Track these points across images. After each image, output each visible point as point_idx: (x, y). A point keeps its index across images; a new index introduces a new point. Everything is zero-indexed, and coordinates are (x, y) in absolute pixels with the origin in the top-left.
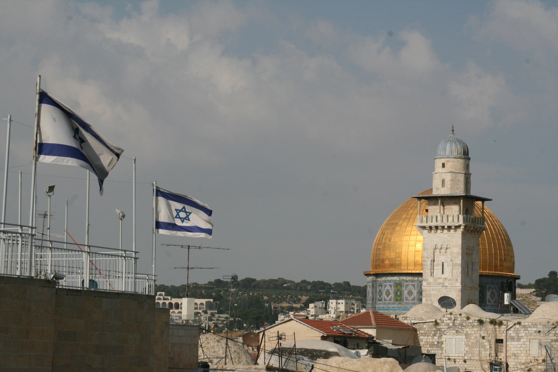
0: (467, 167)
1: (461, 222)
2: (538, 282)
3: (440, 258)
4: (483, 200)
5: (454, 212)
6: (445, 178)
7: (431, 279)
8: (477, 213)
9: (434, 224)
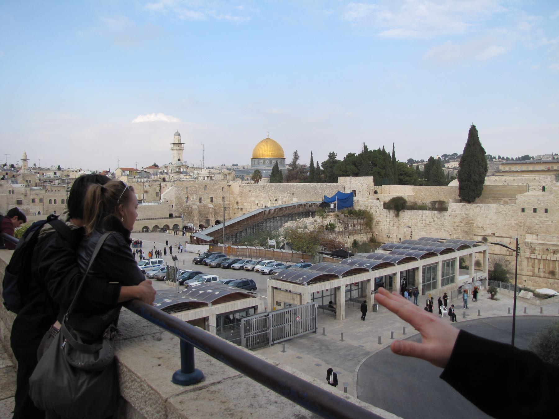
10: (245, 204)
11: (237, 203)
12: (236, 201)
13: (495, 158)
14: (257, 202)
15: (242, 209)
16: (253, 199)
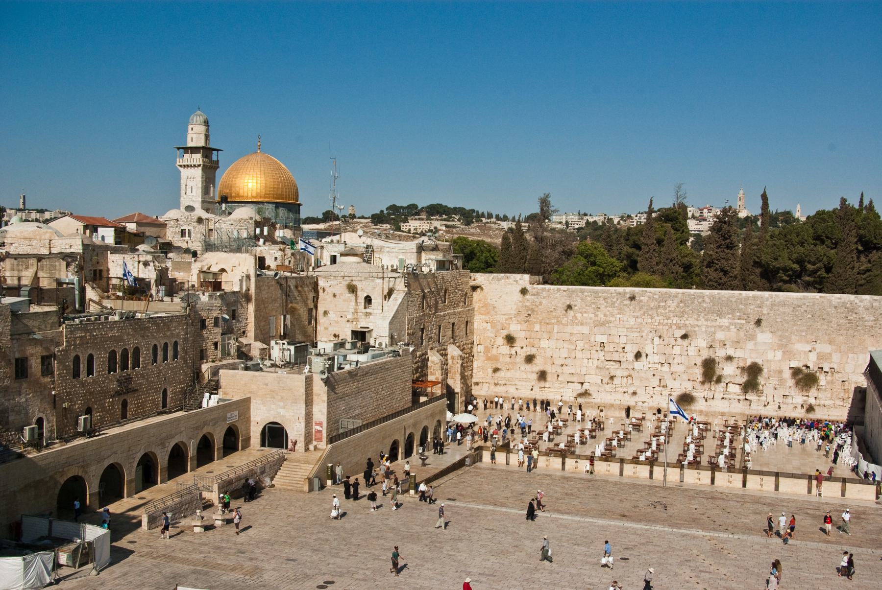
0: (207, 130)
1: (201, 163)
2: (373, 215)
3: (190, 184)
4: (218, 150)
5: (197, 158)
6: (195, 136)
7: (185, 196)
8: (214, 158)
9: (186, 163)
10: (544, 344)
11: (510, 340)
12: (505, 333)
13: (483, 215)
14: (600, 338)
15: (530, 359)
16: (585, 330)
